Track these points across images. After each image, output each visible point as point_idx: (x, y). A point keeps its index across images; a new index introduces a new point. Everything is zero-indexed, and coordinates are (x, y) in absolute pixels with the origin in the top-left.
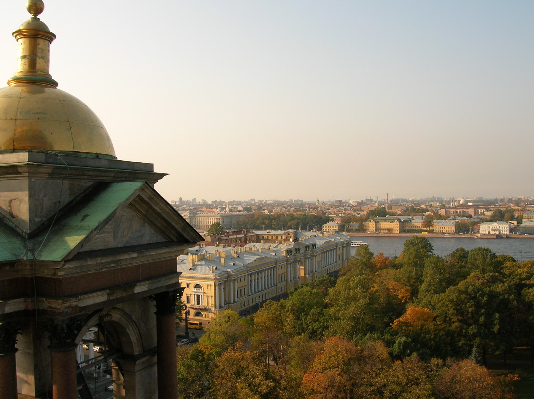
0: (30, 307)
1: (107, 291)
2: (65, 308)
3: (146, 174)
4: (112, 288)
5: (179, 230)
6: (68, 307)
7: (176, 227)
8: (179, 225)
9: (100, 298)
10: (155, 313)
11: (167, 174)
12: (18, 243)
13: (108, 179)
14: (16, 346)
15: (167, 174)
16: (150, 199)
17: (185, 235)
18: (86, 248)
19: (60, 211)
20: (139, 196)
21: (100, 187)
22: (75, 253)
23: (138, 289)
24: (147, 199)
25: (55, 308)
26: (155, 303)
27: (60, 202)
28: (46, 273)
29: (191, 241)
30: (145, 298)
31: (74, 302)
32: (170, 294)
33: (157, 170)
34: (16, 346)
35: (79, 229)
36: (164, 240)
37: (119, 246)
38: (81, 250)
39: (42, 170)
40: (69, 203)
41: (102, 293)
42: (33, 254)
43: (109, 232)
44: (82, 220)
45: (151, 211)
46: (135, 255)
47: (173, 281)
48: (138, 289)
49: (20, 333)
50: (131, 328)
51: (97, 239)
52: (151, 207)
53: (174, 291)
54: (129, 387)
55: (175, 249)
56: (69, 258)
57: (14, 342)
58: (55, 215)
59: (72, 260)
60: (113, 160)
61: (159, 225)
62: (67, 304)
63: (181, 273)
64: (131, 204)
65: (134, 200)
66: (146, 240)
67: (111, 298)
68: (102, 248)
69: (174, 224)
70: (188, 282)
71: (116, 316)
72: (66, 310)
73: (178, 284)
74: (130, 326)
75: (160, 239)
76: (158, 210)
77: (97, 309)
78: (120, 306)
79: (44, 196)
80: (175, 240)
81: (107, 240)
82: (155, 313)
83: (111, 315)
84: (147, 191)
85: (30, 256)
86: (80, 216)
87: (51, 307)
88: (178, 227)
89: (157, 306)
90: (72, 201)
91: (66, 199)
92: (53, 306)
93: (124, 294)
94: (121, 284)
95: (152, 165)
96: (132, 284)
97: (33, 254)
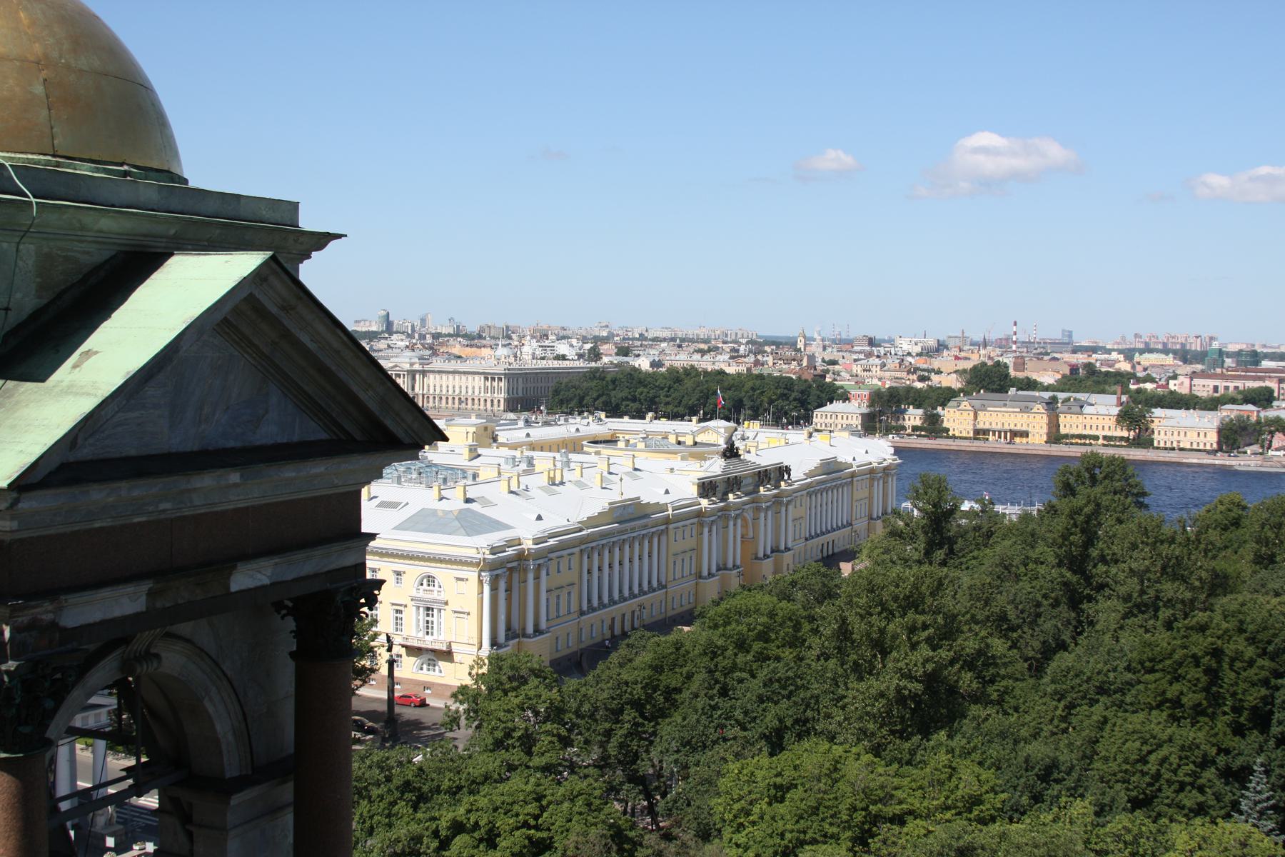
1: (146, 586)
5: (373, 405)
7: (362, 395)
9: (125, 602)
10: (292, 654)
11: (339, 236)
15: (339, 236)
16: (283, 308)
17: (388, 423)
18: (86, 452)
20: (251, 299)
23: (245, 578)
24: (274, 310)
26: (291, 624)
29: (407, 440)
31: (44, 611)
36: (323, 436)
40: (36, 315)
41: (130, 589)
46: (235, 477)
47: (349, 560)
48: (245, 578)
52: (286, 335)
55: (358, 462)
63: (372, 536)
64: (225, 321)
65: (236, 311)
66: (269, 433)
67: (159, 604)
68: (133, 453)
69: (355, 388)
71: (173, 660)
75: (316, 432)
76: (312, 346)
77: (115, 636)
78: (184, 628)
80: (358, 435)
82: (292, 654)
83: (157, 656)
88: (368, 398)
89: (298, 634)
90: (47, 306)
94: (187, 564)
95: (294, 206)
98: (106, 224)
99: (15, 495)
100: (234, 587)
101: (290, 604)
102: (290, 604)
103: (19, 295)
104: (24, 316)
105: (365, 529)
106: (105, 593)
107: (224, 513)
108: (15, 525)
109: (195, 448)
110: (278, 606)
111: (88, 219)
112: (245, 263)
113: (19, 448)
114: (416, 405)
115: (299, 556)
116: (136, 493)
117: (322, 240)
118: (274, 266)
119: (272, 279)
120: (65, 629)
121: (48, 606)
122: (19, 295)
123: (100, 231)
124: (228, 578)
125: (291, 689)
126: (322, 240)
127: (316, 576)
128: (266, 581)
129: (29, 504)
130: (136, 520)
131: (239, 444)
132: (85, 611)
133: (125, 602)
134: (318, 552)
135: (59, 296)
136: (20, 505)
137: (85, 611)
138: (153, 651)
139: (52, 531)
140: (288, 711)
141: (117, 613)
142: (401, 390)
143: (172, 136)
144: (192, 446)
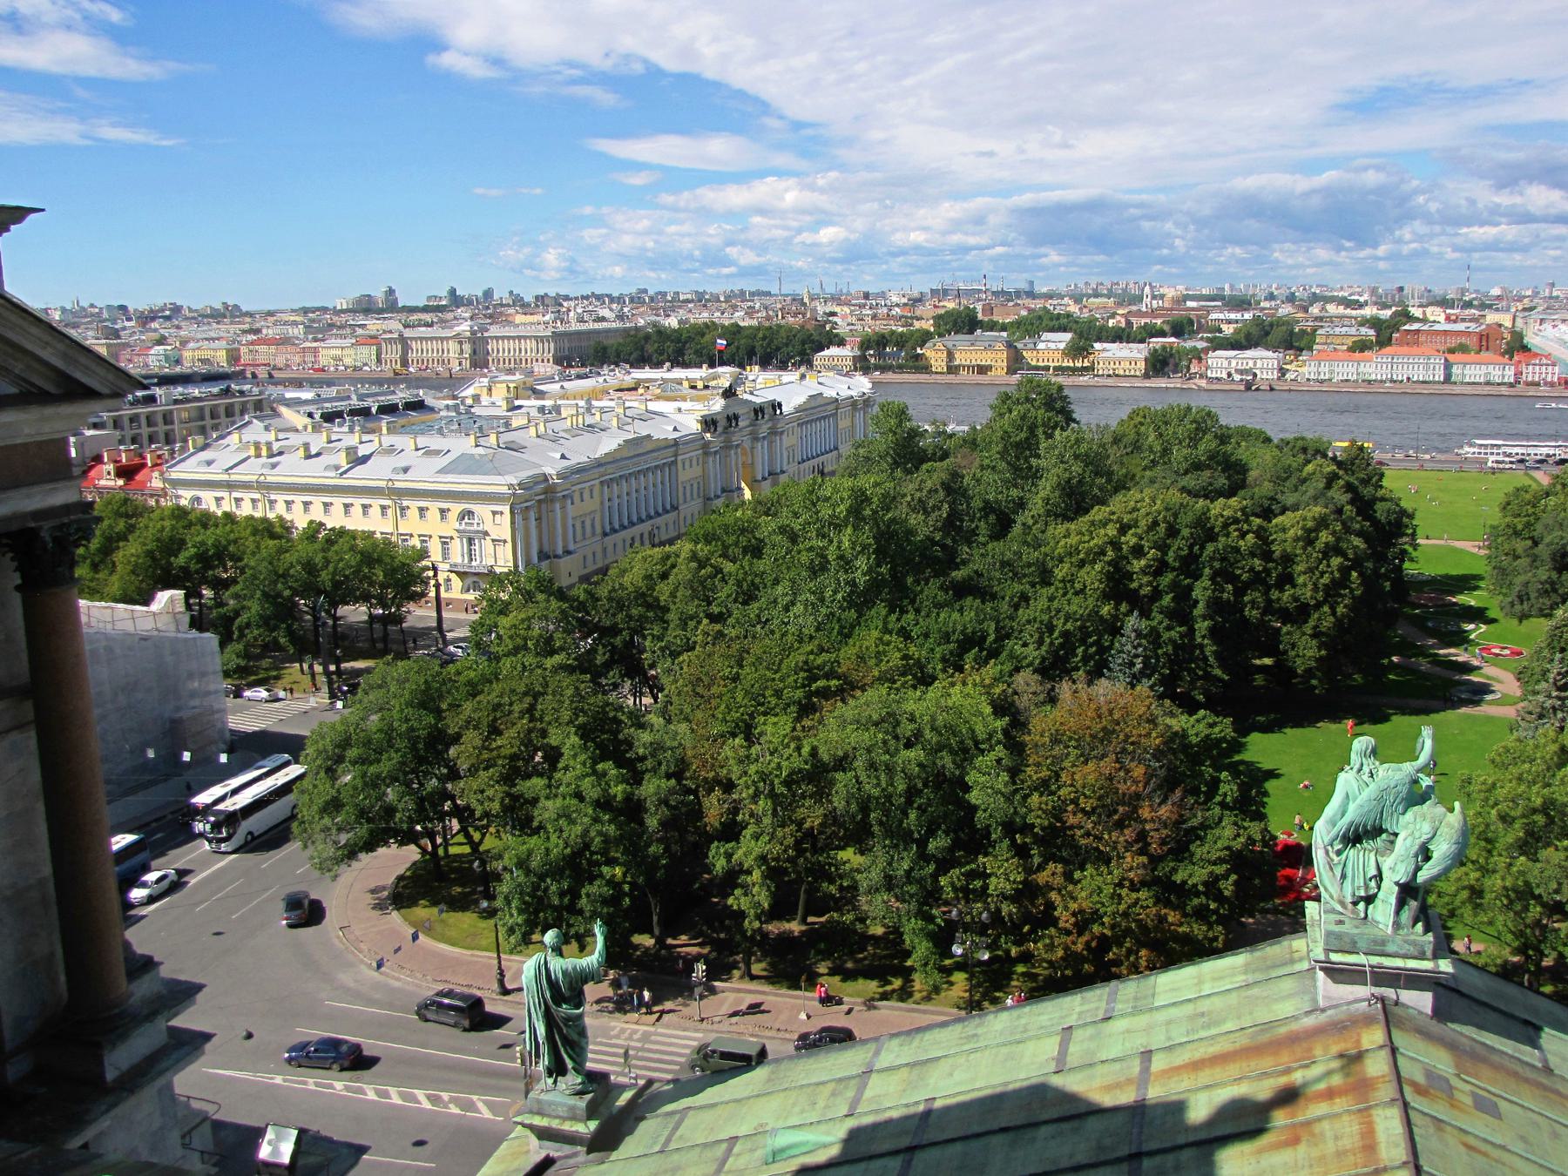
5: (58, 362)
10: (18, 588)
17: (78, 375)
29: (105, 391)
36: (13, 390)
80: (51, 388)
82: (18, 588)
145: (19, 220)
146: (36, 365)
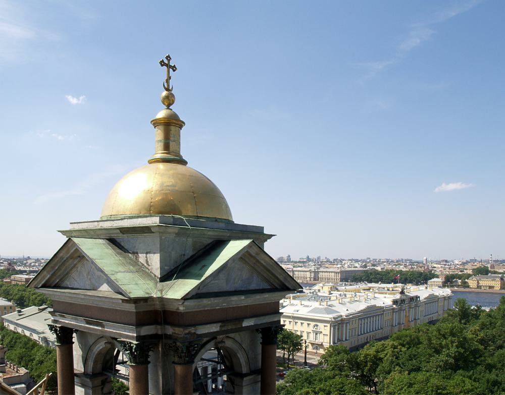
0: (160, 333)
1: (219, 324)
2: (185, 334)
3: (257, 235)
4: (223, 321)
6: (188, 334)
7: (279, 277)
8: (281, 276)
9: (214, 328)
10: (261, 343)
11: (275, 235)
12: (151, 284)
13: (225, 238)
14: (149, 360)
15: (275, 235)
16: (256, 254)
18: (204, 291)
19: (184, 262)
20: (247, 252)
21: (218, 244)
22: (194, 293)
23: (246, 323)
25: (178, 334)
26: (260, 335)
27: (184, 255)
28: (172, 308)
30: (254, 329)
31: (192, 330)
32: (273, 329)
33: (266, 232)
34: (149, 360)
35: (198, 277)
36: (269, 287)
37: (231, 290)
38: (199, 292)
39: (170, 230)
40: (192, 256)
41: (215, 325)
42: (162, 293)
43: (223, 279)
44: (201, 269)
45: (258, 264)
46: (243, 297)
47: (276, 320)
48: (246, 323)
49: (152, 351)
50: (241, 353)
51: (213, 284)
52: (258, 261)
53: (276, 327)
54: (142, 381)
56: (187, 297)
57: (148, 356)
58: (180, 265)
59: (192, 298)
60: (230, 223)
61: (265, 275)
62: (187, 331)
63: (283, 313)
64: (241, 258)
65: (244, 255)
66: (253, 286)
67: (223, 329)
68: (216, 291)
69: (277, 275)
70: (285, 319)
71: (229, 343)
72: (185, 336)
73: (279, 321)
74: (240, 351)
75: (266, 286)
76: (264, 264)
77: (213, 337)
78: (232, 335)
79: (172, 251)
81: (222, 285)
82: (261, 343)
83: (224, 342)
84: (254, 248)
85: (159, 295)
86: (199, 266)
87: (175, 333)
88: (281, 278)
90: (195, 254)
91: (190, 253)
92: (177, 332)
93: (234, 327)
94: (231, 320)
95: (263, 227)
96: (241, 319)
97: (162, 293)
98: (209, 233)
99: (183, 301)
100: (243, 326)
101: (260, 330)
102: (260, 330)
103: (188, 252)
104: (189, 256)
105: (280, 311)
106: (208, 326)
107: (241, 306)
108: (184, 308)
109: (233, 290)
110: (257, 330)
111: (205, 232)
112: (245, 243)
113: (184, 289)
114: (293, 279)
115: (262, 318)
116: (216, 301)
117: (270, 236)
118: (253, 243)
119: (253, 246)
120: (198, 335)
121: (193, 328)
122: (188, 252)
123: (209, 235)
124: (242, 323)
125: (261, 352)
126: (270, 236)
127: (267, 323)
128: (253, 324)
129: (187, 303)
130: (217, 308)
131: (245, 289)
132: (203, 330)
133: (214, 328)
134: (267, 317)
135: (198, 252)
136: (185, 303)
137: (203, 330)
138: (224, 341)
139: (194, 310)
140: (260, 357)
141: (212, 331)
142: (290, 276)
143: (230, 210)
144: (233, 289)
145: (270, 238)
146: (276, 280)
